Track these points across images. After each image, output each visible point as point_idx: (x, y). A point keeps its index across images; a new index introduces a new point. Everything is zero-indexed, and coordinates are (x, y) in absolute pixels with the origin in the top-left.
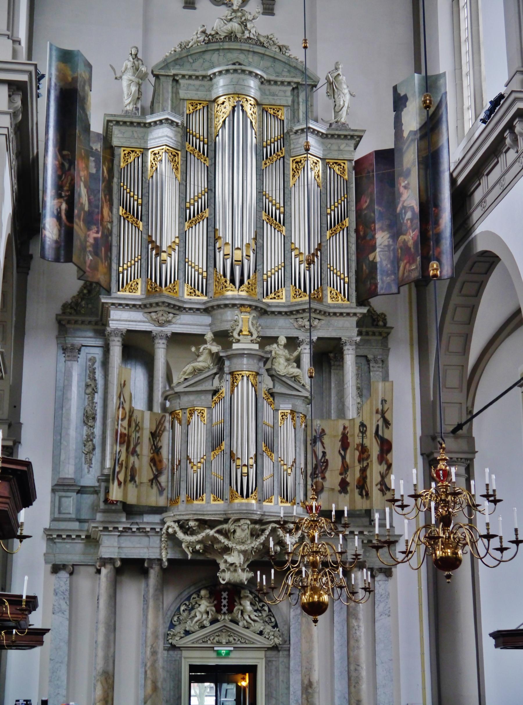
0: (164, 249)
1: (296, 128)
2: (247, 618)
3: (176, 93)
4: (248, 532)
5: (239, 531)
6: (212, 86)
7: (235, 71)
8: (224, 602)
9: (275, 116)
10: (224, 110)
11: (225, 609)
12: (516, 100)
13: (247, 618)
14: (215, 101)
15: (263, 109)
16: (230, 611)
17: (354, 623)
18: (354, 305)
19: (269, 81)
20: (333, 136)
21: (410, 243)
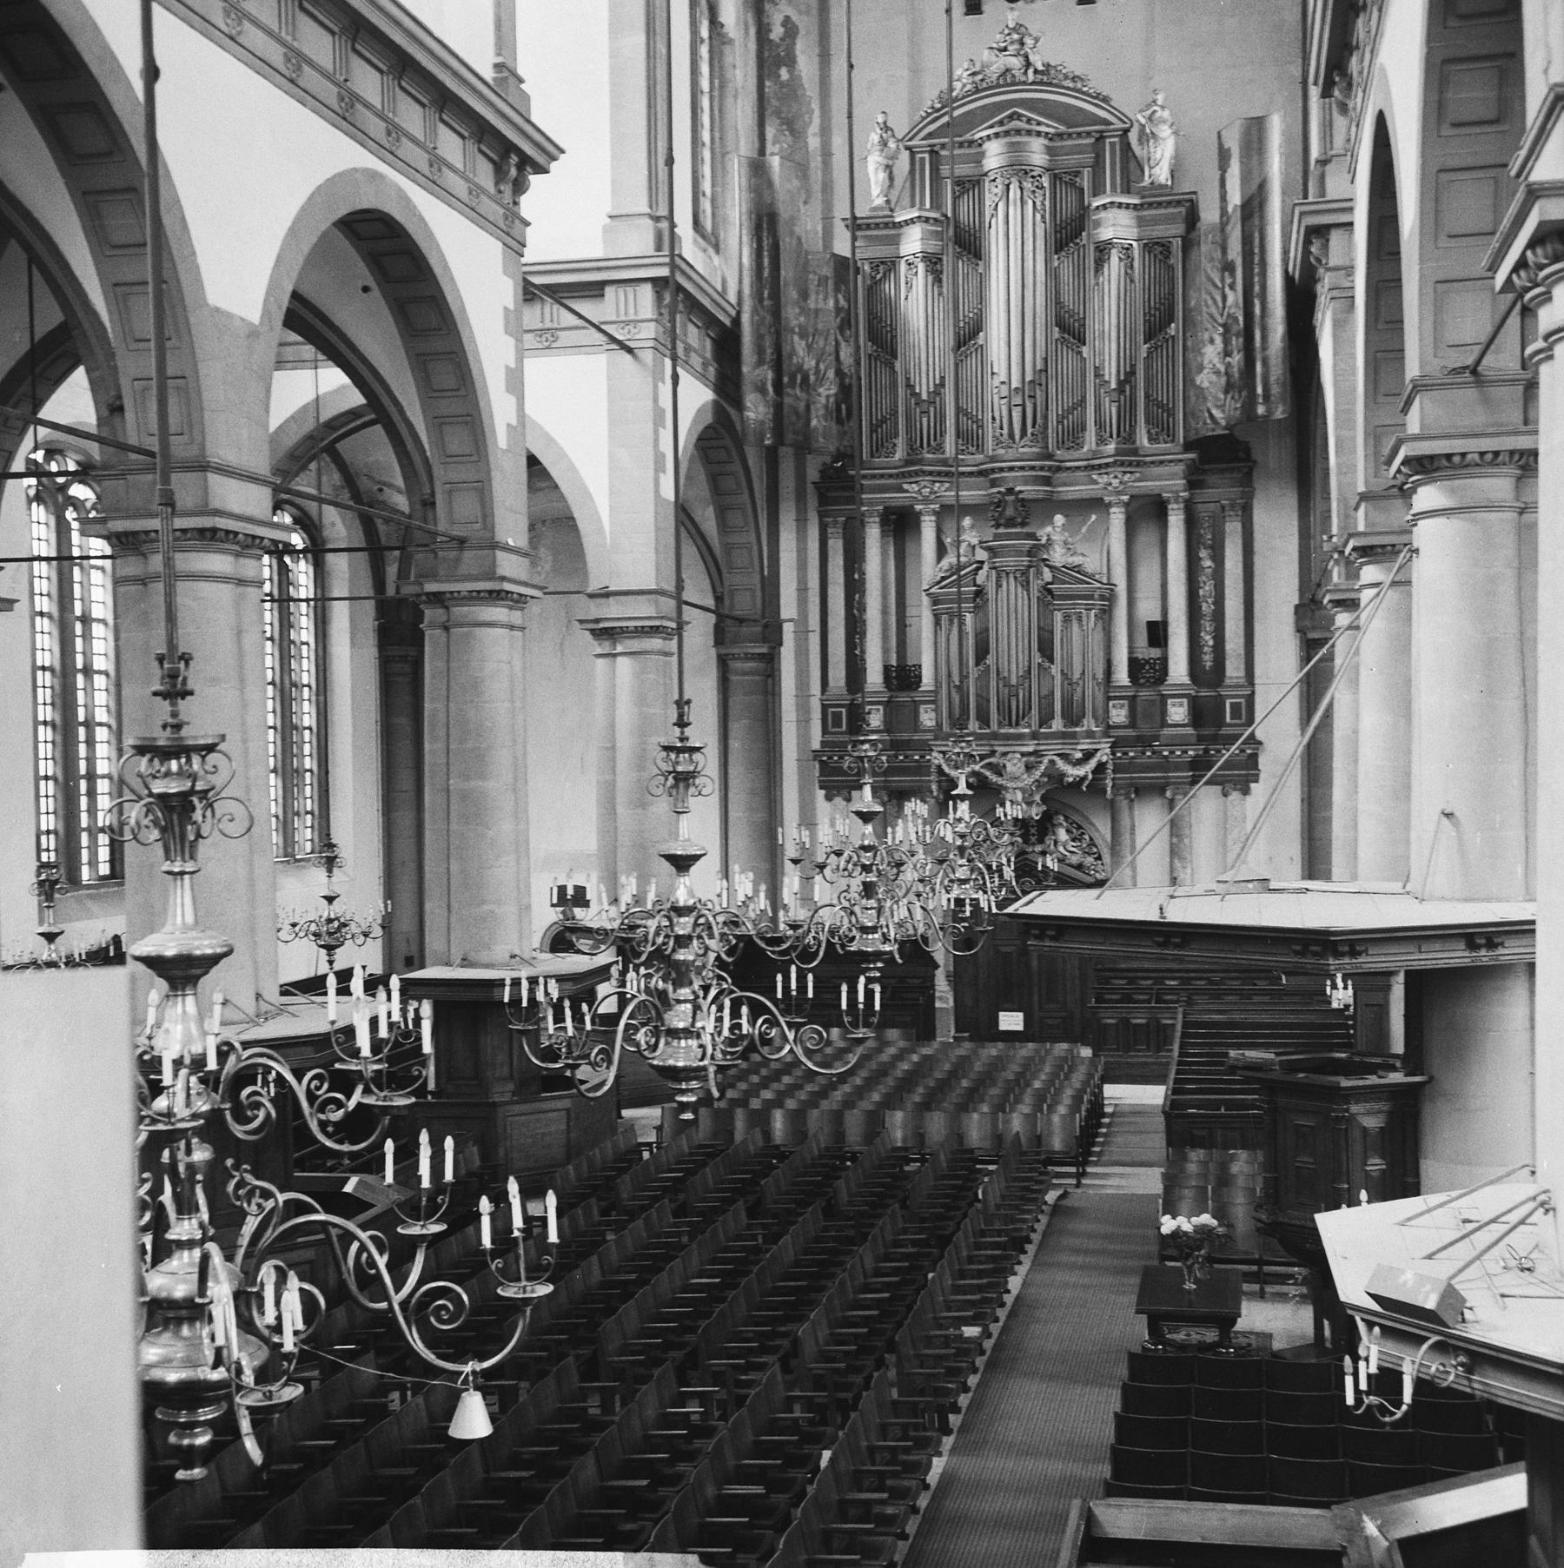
0: (924, 396)
1: (1095, 204)
2: (1061, 849)
3: (935, 170)
4: (1021, 766)
5: (1009, 765)
6: (982, 154)
7: (1007, 133)
8: (1033, 831)
9: (1073, 184)
10: (995, 190)
11: (1033, 839)
12: (1302, 214)
13: (1061, 849)
14: (986, 175)
15: (1055, 176)
16: (1041, 841)
17: (1177, 863)
18: (1179, 449)
19: (1060, 136)
20: (1150, 205)
21: (1235, 371)
